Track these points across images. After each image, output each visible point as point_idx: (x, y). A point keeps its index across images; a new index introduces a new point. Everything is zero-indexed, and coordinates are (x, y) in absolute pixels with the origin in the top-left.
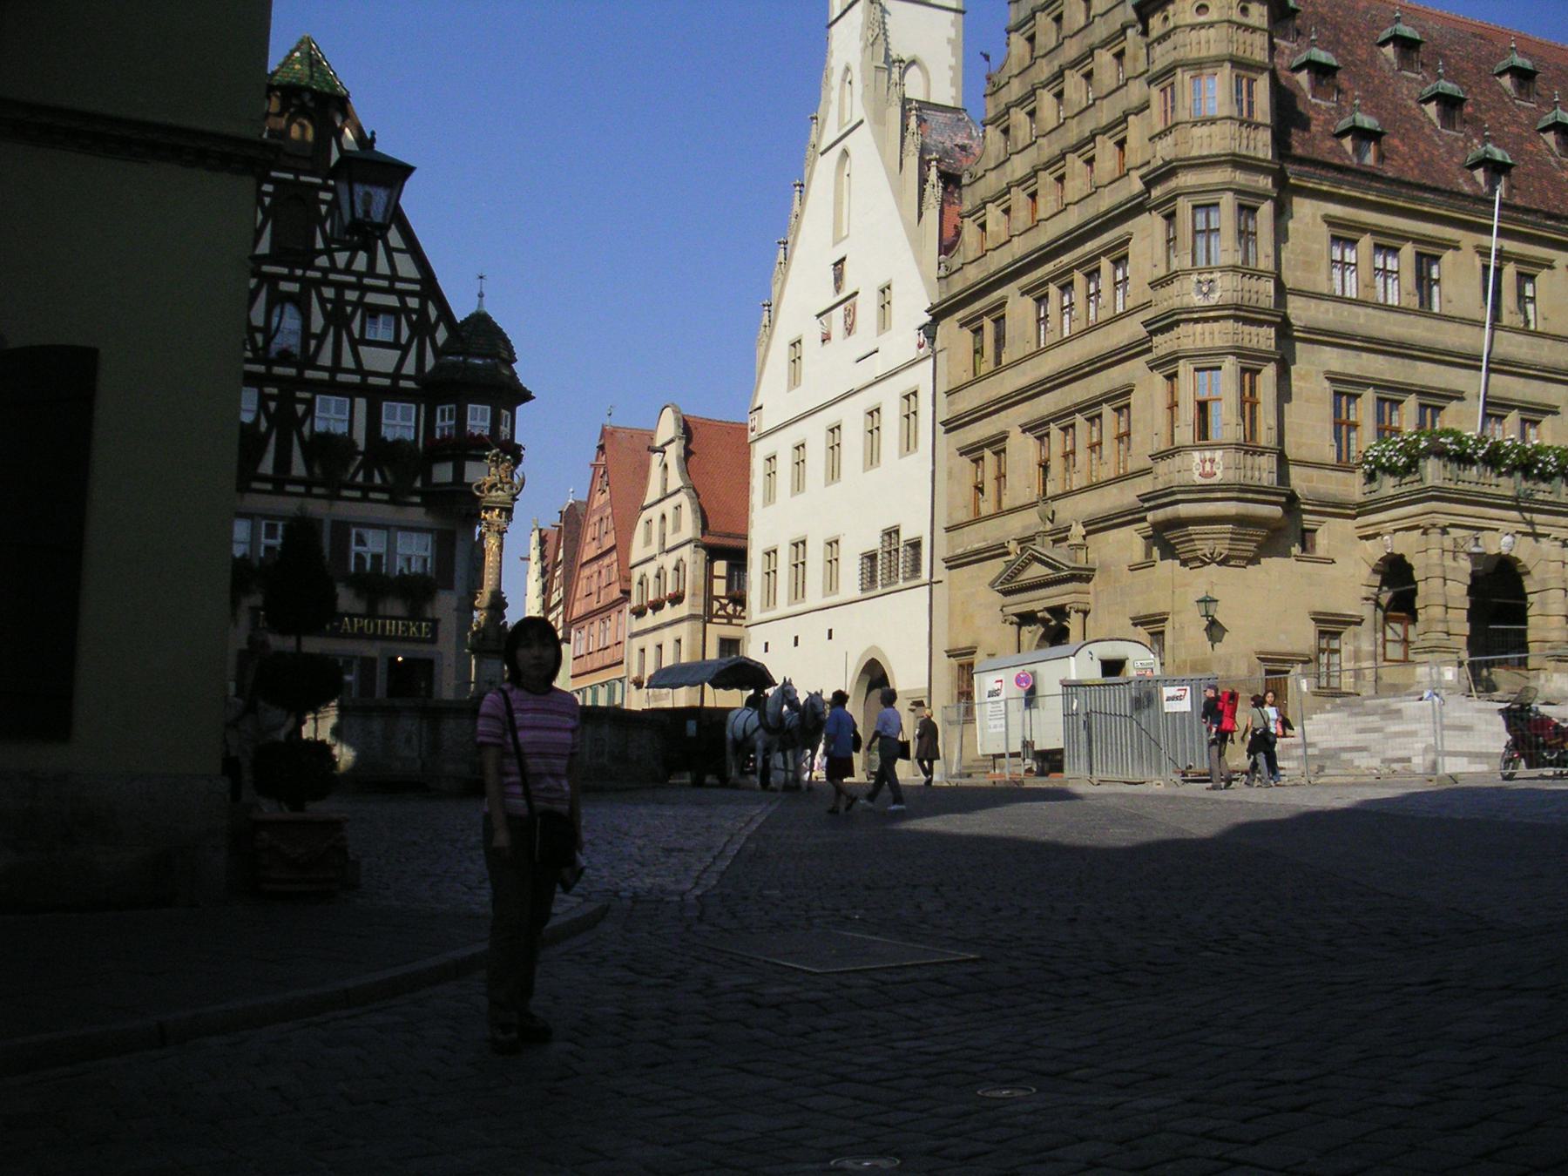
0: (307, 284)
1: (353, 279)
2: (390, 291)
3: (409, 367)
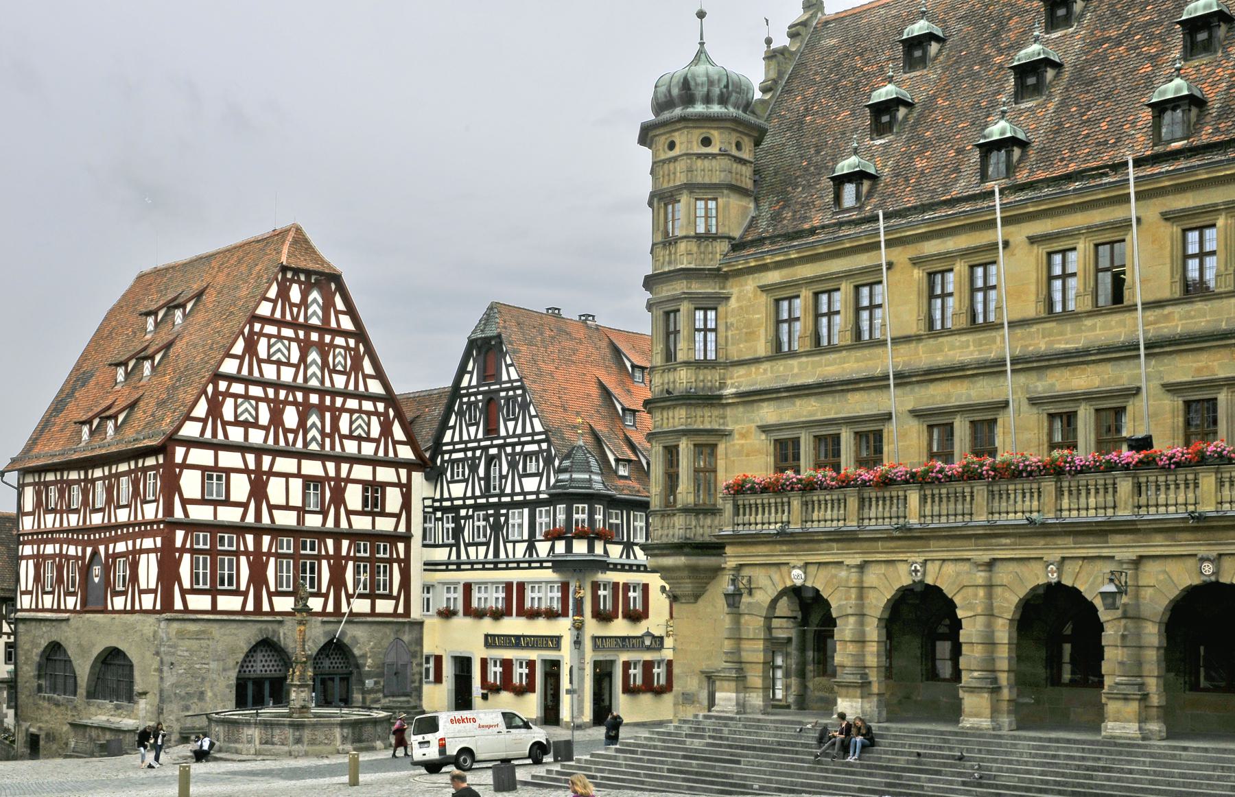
0: (501, 447)
1: (516, 440)
2: (532, 442)
3: (543, 487)
